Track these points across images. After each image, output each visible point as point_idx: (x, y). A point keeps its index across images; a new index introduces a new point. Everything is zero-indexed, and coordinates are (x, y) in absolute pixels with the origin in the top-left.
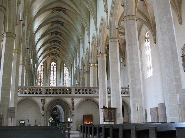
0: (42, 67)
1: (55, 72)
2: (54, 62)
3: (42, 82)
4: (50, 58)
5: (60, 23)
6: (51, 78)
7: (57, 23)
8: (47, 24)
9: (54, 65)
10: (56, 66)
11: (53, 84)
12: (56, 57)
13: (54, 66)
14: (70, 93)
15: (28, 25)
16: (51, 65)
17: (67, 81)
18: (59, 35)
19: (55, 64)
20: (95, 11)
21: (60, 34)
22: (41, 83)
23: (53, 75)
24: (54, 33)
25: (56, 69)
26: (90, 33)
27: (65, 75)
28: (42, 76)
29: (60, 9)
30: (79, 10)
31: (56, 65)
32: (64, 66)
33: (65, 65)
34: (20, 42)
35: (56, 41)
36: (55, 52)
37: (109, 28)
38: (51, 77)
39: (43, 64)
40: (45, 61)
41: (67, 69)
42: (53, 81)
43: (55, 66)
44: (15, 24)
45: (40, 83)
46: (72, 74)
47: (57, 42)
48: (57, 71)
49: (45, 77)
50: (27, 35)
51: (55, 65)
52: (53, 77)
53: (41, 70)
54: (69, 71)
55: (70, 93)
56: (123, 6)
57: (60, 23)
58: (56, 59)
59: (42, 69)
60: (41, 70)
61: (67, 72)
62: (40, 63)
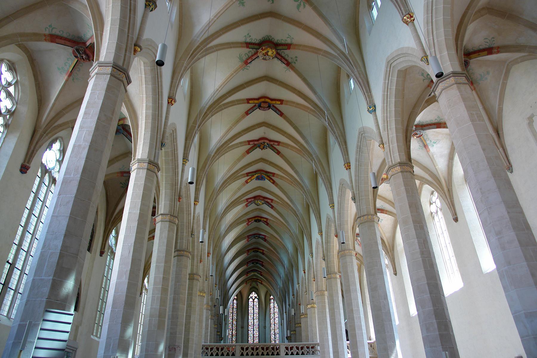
0: (235, 302)
1: (256, 311)
2: (254, 293)
3: (234, 328)
4: (248, 287)
5: (261, 236)
6: (251, 321)
7: (256, 238)
8: (240, 241)
9: (253, 298)
10: (258, 299)
11: (254, 331)
12: (257, 285)
13: (254, 300)
14: (278, 354)
15: (214, 249)
16: (250, 297)
17: (276, 324)
18: (260, 252)
19: (256, 295)
20: (308, 224)
21: (261, 263)
22: (232, 331)
23: (254, 315)
24: (252, 250)
25: (258, 304)
26: (304, 255)
27: (272, 315)
28: (235, 317)
29: (259, 218)
30: (286, 221)
31: (257, 297)
32: (270, 299)
33: (272, 297)
34: (205, 280)
35: (256, 261)
36: (254, 277)
37: (326, 258)
38: (250, 318)
39: (236, 297)
40: (240, 292)
41: (276, 305)
42: (253, 327)
43: (256, 300)
44: (199, 261)
45: (232, 329)
46: (285, 314)
47: (257, 263)
48: (259, 308)
49: (240, 320)
50: (212, 263)
51: (256, 297)
52: (254, 319)
53: (233, 308)
54: (279, 308)
55: (278, 353)
56: (336, 236)
57: (261, 236)
58: (257, 287)
59: (235, 305)
60: (233, 308)
61: (277, 310)
62: (232, 296)
